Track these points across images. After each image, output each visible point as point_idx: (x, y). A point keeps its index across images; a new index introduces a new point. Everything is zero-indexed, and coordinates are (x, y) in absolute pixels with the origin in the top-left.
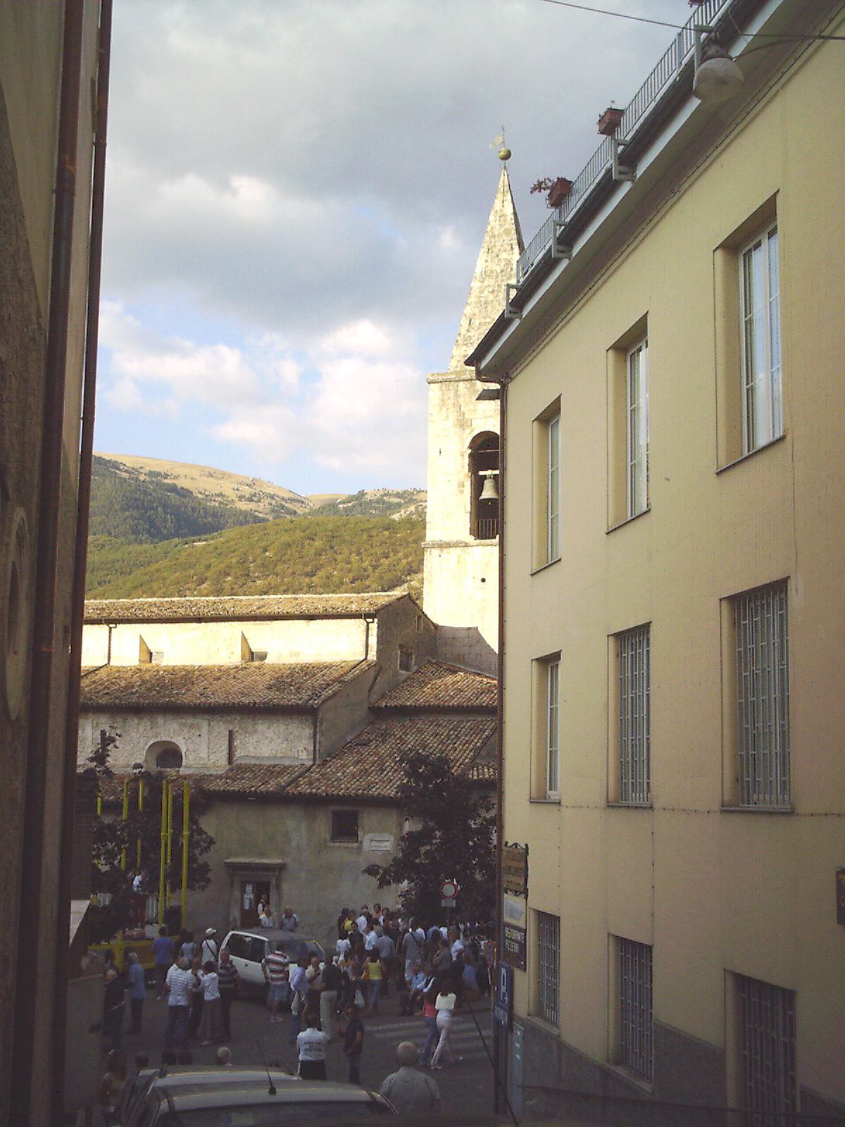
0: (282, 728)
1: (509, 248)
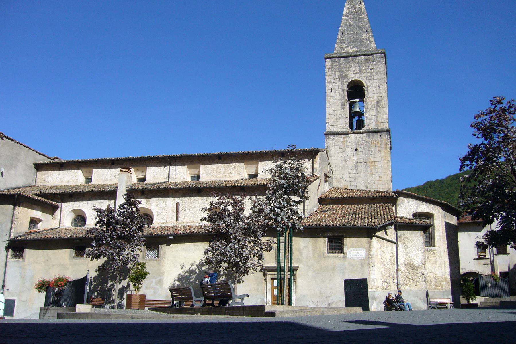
1: (359, 3)
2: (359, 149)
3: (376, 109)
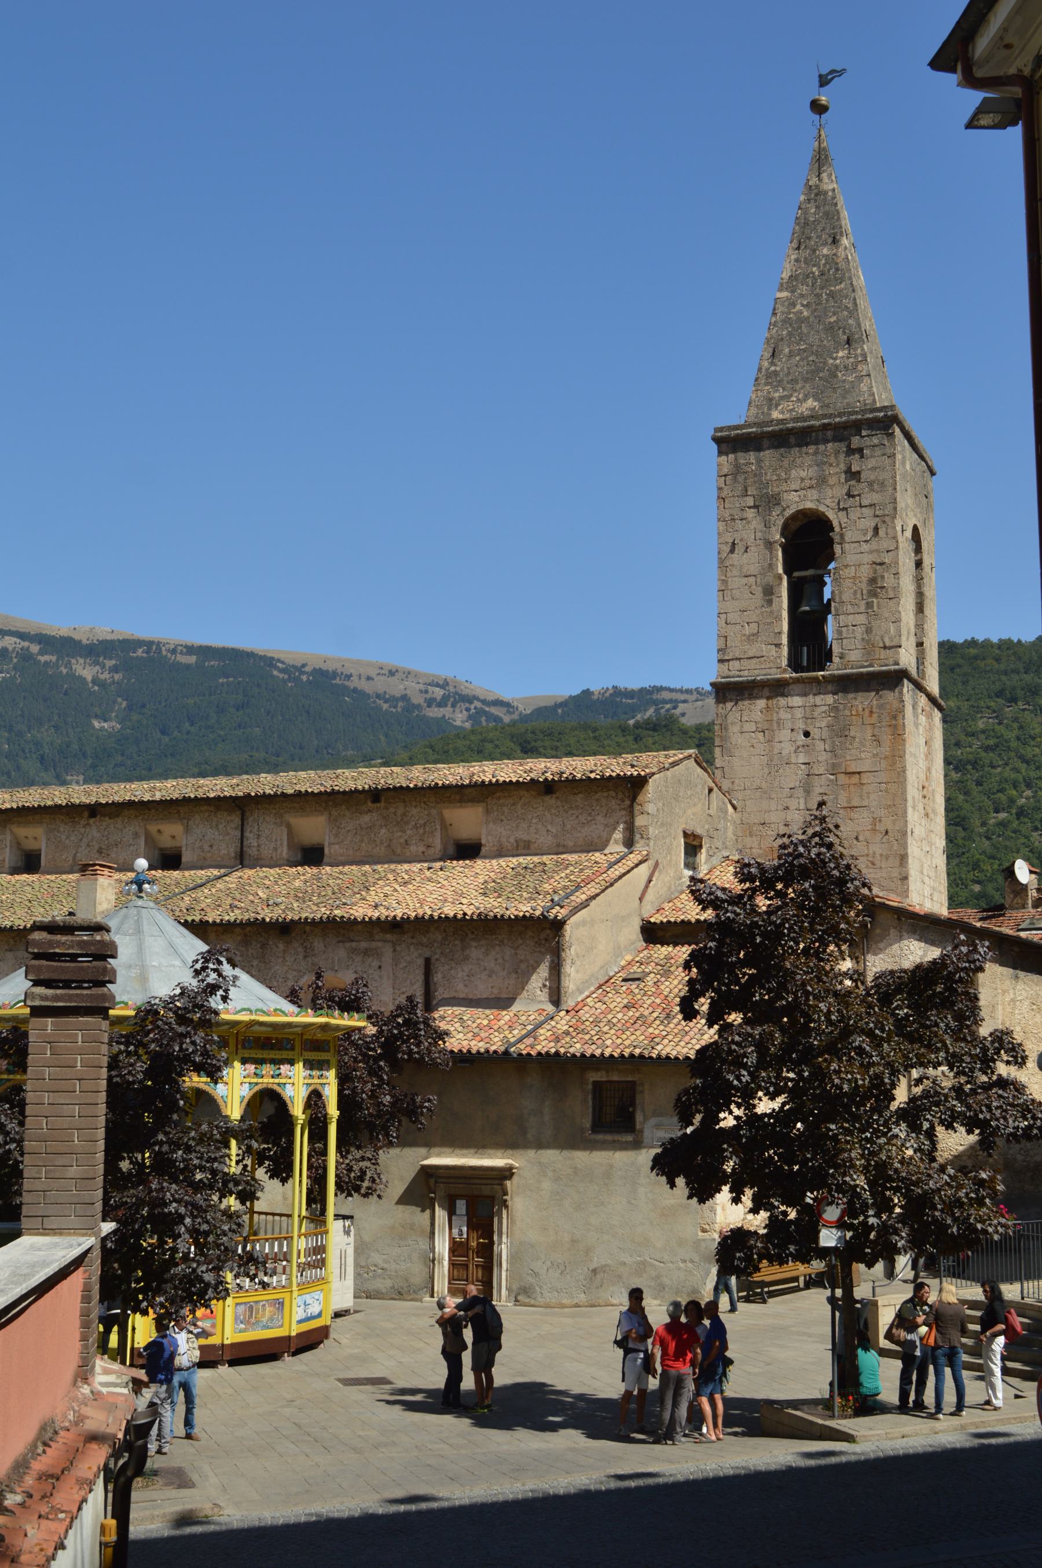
0: (508, 952)
1: (830, 240)
2: (815, 733)
3: (867, 603)
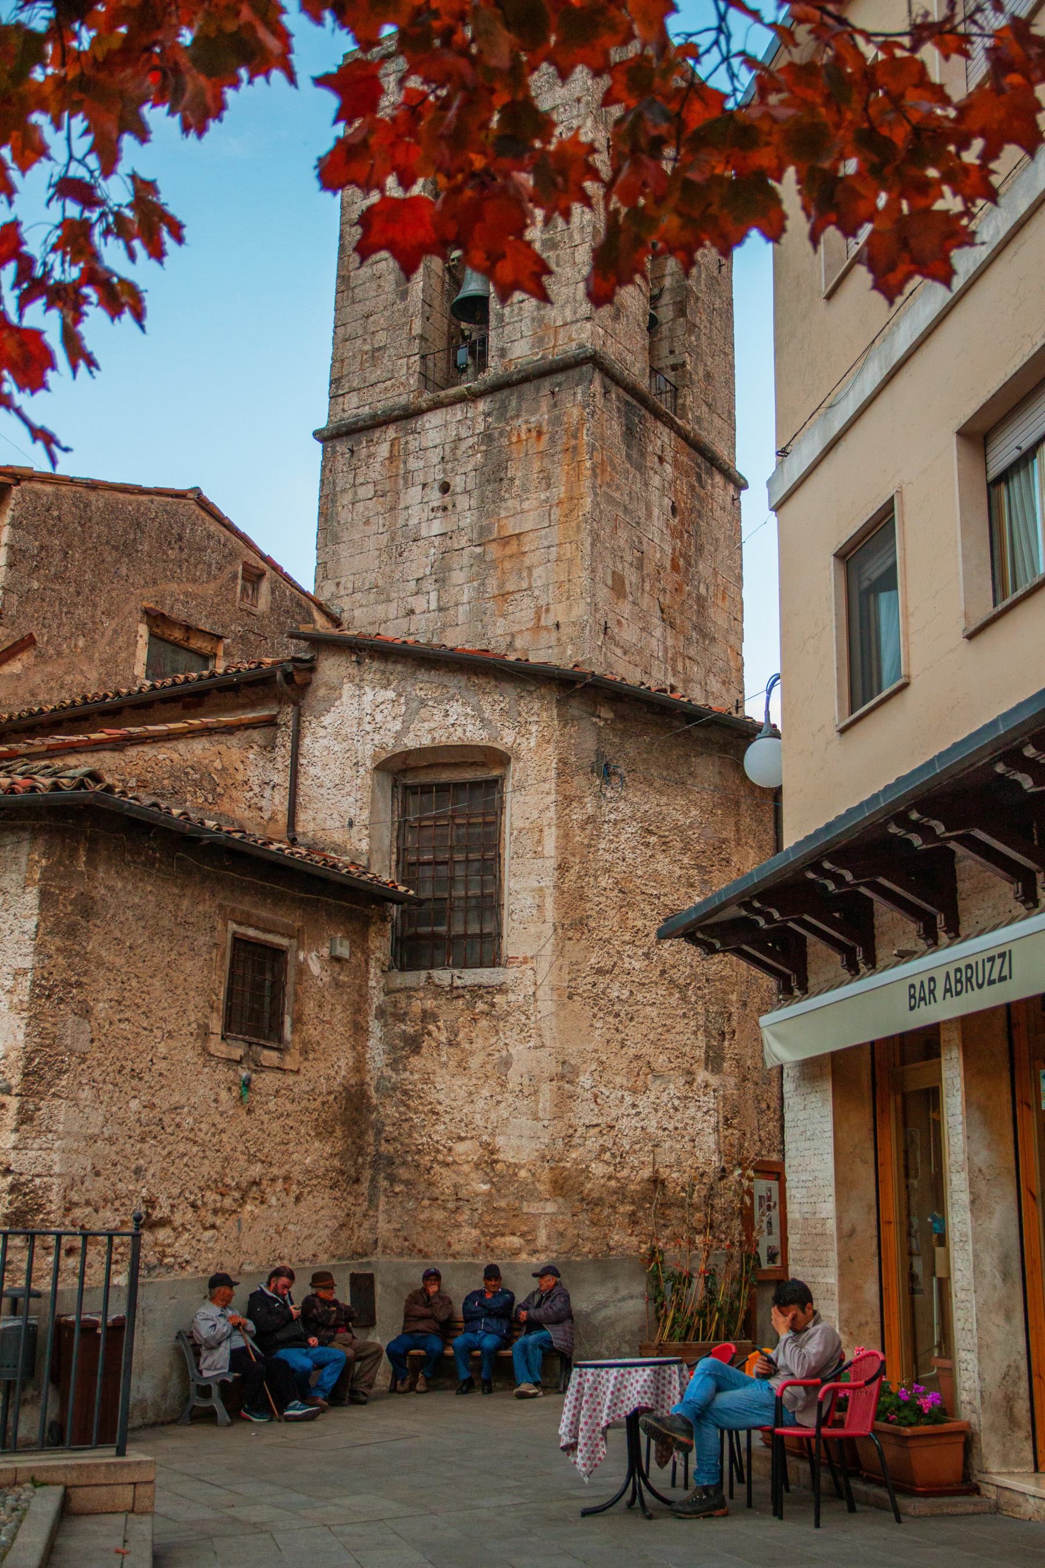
2: (458, 483)
